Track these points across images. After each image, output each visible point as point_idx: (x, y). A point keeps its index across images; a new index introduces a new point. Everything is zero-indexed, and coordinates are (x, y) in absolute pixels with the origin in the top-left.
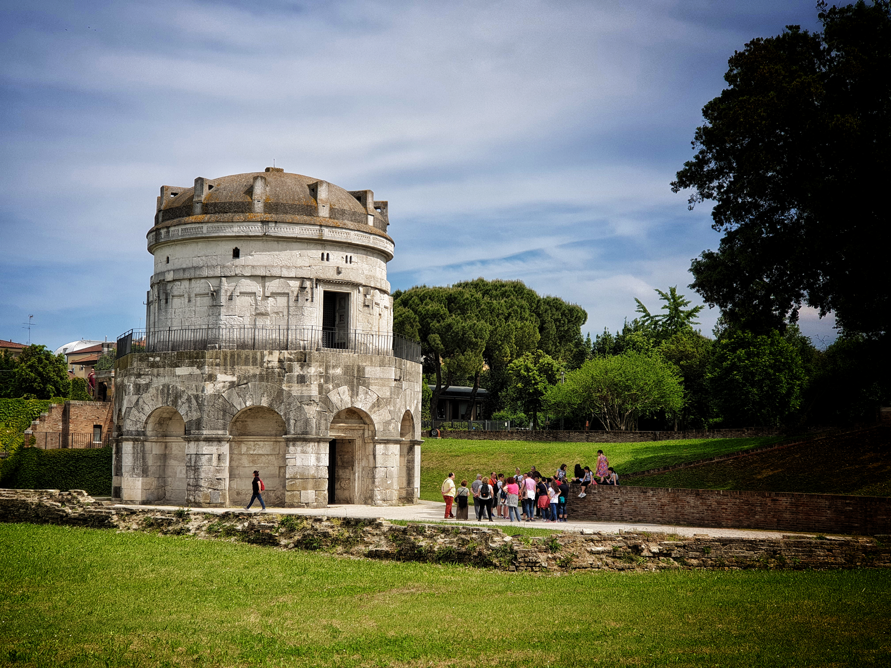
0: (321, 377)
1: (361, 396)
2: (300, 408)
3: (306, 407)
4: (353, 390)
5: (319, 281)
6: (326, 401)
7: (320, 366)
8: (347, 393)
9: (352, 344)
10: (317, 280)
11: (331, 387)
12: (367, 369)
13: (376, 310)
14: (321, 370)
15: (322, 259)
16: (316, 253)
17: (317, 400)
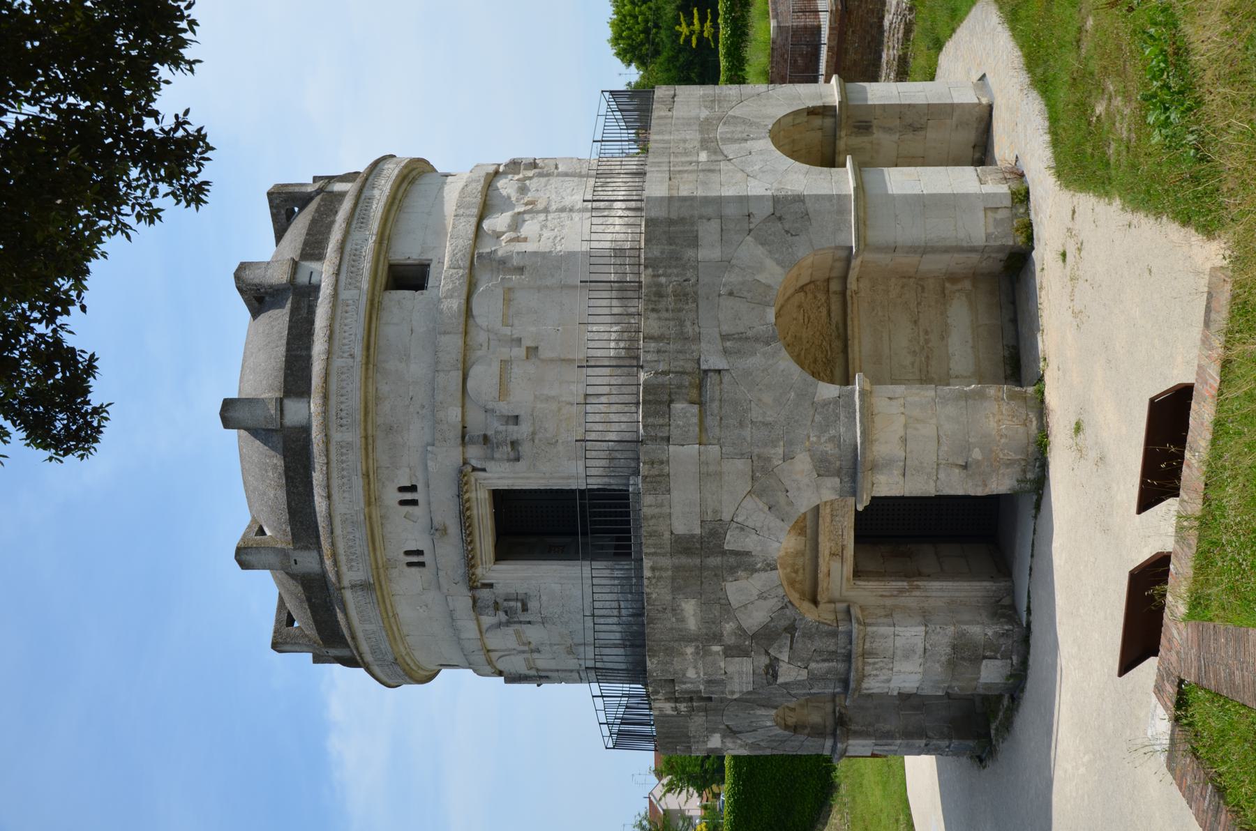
0: (707, 653)
1: (749, 542)
2: (786, 685)
3: (780, 680)
4: (732, 570)
5: (473, 585)
6: (766, 637)
7: (683, 654)
8: (742, 583)
9: (615, 483)
10: (472, 588)
11: (729, 627)
12: (680, 528)
13: (521, 398)
14: (690, 650)
15: (422, 564)
16: (407, 586)
17: (764, 660)
